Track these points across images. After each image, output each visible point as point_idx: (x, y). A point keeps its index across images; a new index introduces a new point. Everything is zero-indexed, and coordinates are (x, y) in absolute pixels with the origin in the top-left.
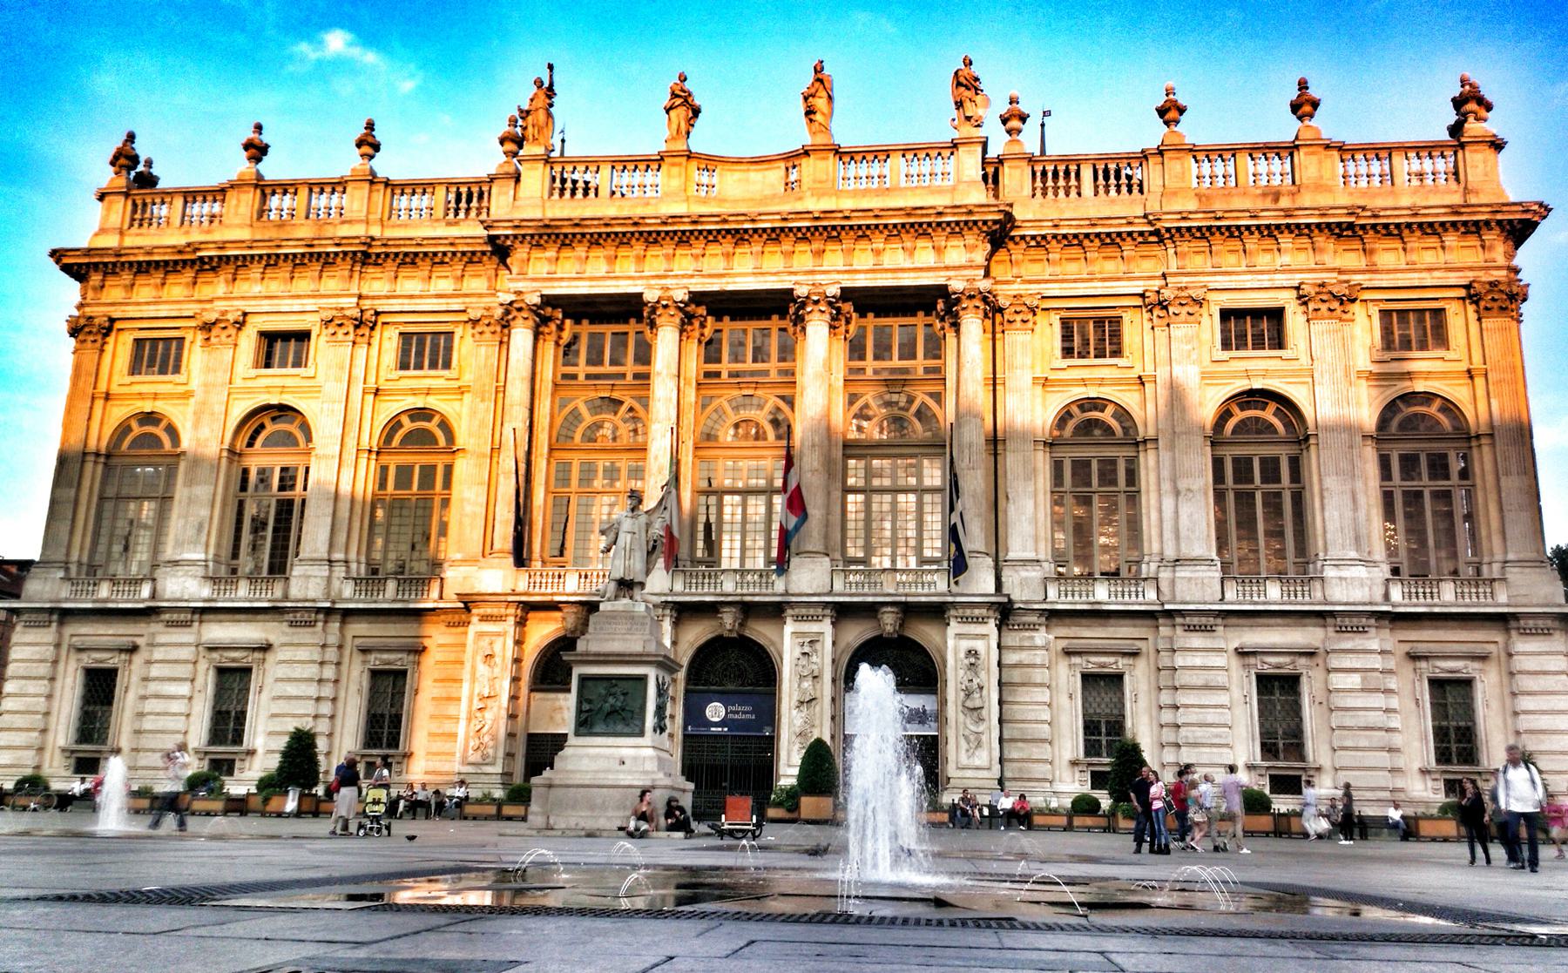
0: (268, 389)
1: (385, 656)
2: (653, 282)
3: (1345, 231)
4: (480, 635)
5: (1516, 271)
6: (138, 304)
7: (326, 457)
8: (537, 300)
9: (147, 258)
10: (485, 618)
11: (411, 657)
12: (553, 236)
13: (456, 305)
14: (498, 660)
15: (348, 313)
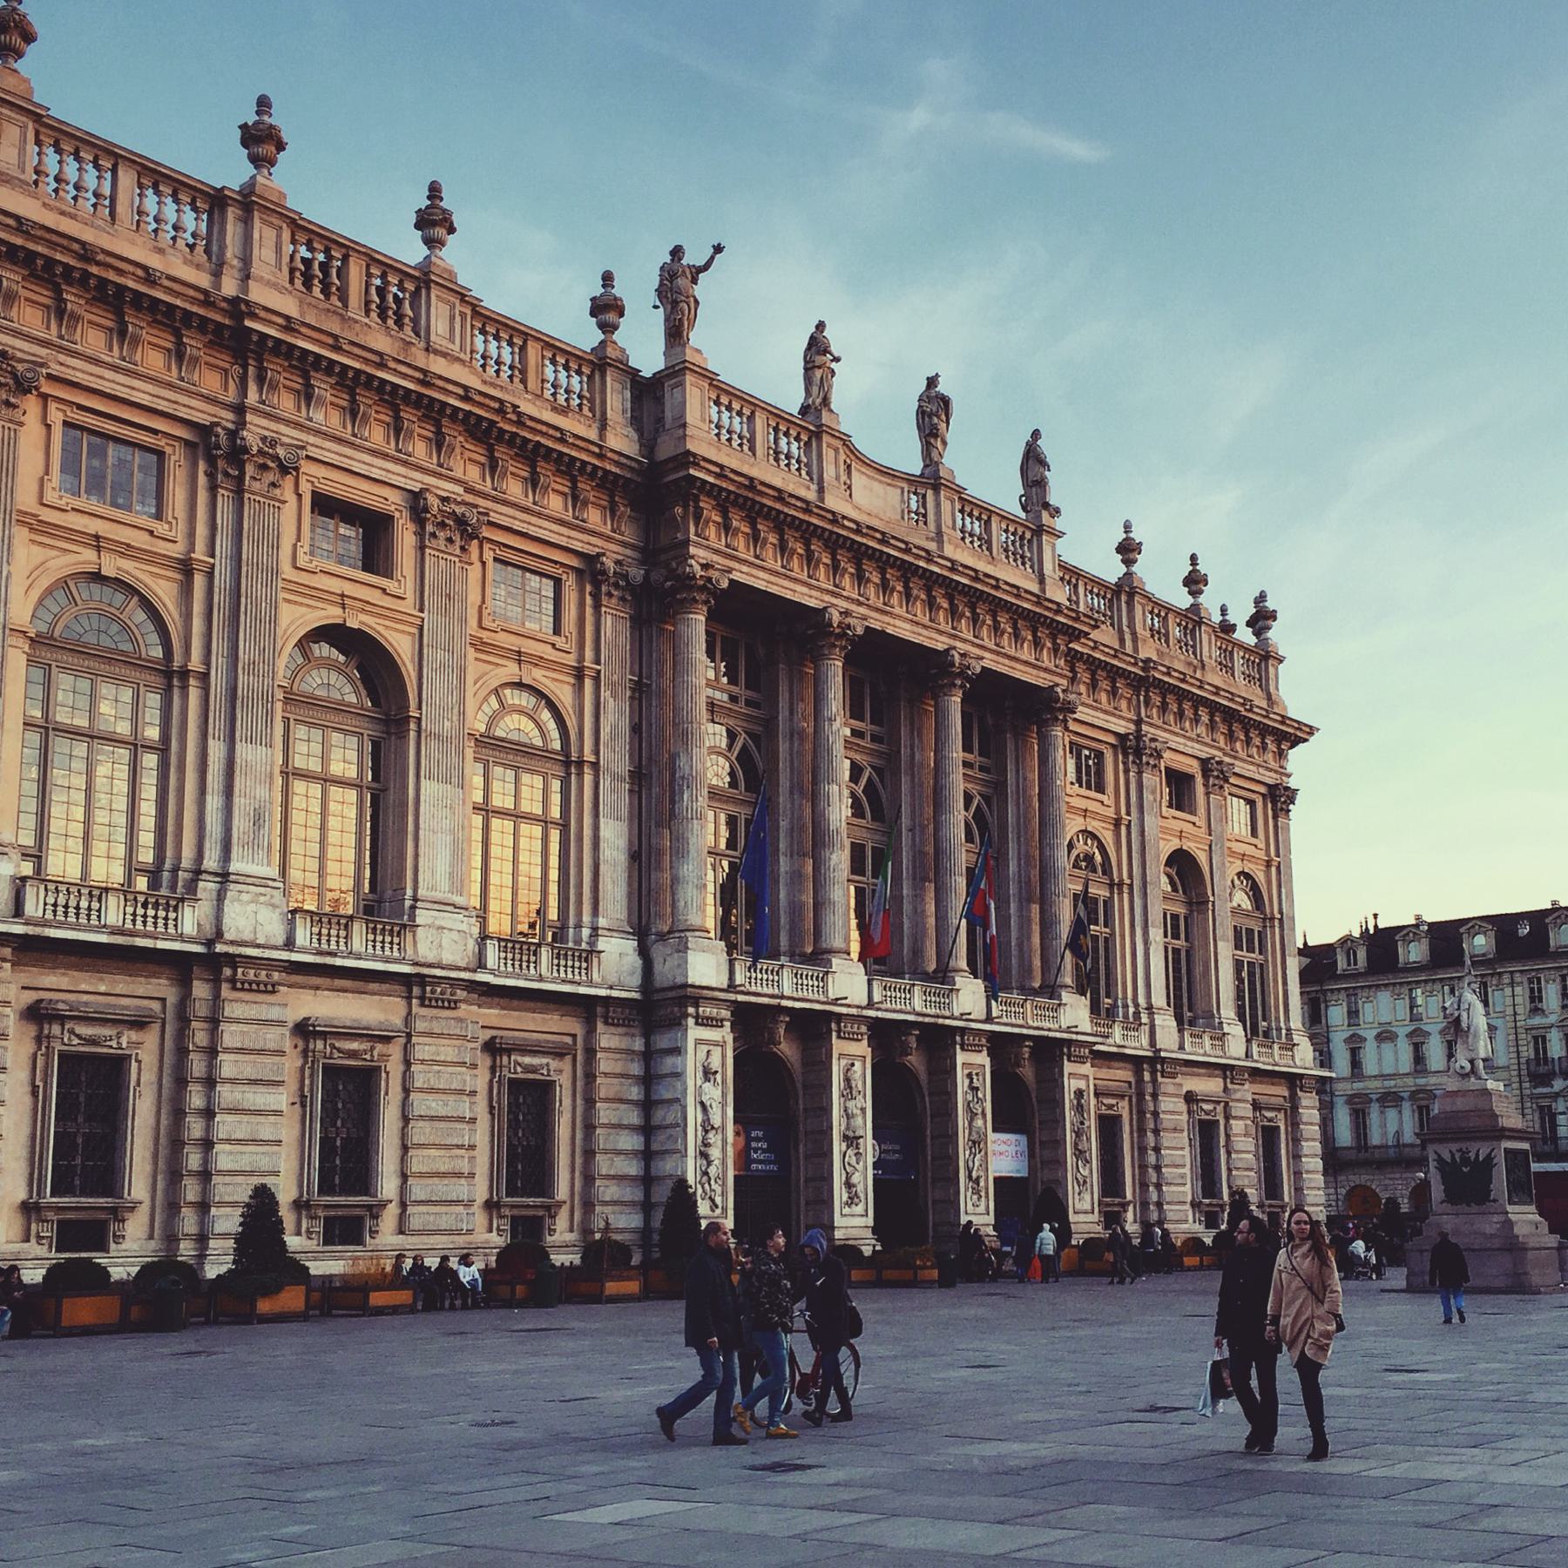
0: (343, 600)
1: (527, 1060)
2: (827, 598)
3: (1230, 716)
4: (698, 1042)
5: (1289, 776)
6: (97, 362)
7: (438, 737)
8: (725, 584)
9: (142, 289)
10: (702, 1021)
11: (554, 1064)
12: (749, 505)
13: (579, 542)
14: (719, 1077)
15: (459, 510)
